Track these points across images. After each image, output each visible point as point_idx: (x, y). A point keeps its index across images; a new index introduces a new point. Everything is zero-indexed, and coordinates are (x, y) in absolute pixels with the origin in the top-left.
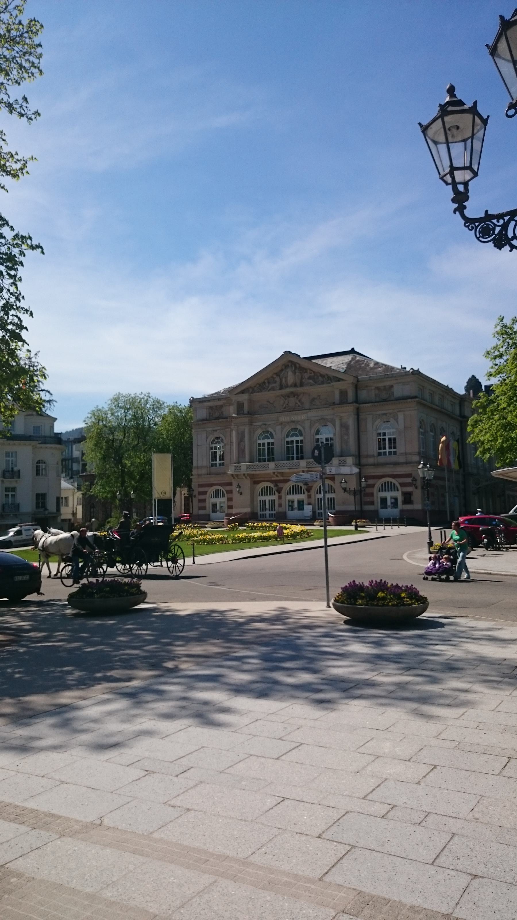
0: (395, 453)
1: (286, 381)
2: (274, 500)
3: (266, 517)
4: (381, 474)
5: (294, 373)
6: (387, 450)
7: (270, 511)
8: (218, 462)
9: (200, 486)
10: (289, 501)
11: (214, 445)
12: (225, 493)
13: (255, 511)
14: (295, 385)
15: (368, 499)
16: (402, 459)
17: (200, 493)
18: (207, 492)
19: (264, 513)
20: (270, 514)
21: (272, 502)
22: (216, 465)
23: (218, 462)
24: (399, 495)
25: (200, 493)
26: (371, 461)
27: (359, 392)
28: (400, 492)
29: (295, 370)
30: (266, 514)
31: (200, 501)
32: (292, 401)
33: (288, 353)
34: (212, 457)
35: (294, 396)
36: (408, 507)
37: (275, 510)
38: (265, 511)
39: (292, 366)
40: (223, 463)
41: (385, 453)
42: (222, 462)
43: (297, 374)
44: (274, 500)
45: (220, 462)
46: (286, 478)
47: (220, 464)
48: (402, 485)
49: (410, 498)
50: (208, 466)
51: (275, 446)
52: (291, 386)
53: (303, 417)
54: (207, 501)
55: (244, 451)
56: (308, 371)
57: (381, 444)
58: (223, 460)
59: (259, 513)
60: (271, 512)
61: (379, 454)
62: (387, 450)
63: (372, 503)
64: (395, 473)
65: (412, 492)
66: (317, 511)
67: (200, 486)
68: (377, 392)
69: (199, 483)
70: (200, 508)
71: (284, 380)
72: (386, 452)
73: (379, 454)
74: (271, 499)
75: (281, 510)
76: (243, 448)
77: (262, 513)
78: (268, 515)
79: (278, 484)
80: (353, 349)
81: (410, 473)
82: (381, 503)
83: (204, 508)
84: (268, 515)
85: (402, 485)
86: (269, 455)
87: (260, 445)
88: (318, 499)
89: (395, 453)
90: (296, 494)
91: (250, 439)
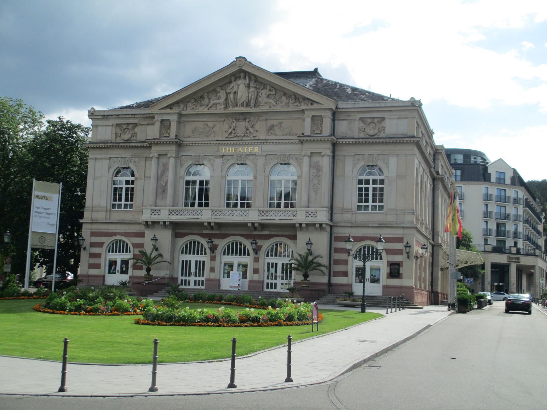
0: (381, 208)
1: (235, 98)
2: (204, 262)
3: (189, 284)
4: (361, 235)
5: (248, 87)
6: (370, 203)
7: (196, 276)
8: (123, 202)
9: (93, 234)
10: (225, 265)
12: (130, 245)
13: (175, 276)
14: (248, 105)
15: (340, 268)
16: (391, 219)
17: (93, 245)
18: (103, 243)
19: (187, 278)
20: (195, 281)
21: (200, 265)
22: (120, 206)
23: (123, 202)
24: (382, 265)
25: (93, 245)
26: (347, 217)
27: (336, 122)
28: (385, 261)
29: (249, 84)
30: (189, 281)
31: (92, 255)
32: (241, 126)
33: (241, 59)
34: (115, 194)
35: (245, 120)
37: (203, 276)
38: (189, 276)
39: (245, 78)
40: (131, 205)
41: (367, 207)
42: (129, 203)
43: (252, 89)
44: (204, 262)
45: (126, 203)
46: (223, 232)
47: (126, 206)
48: (389, 252)
49: (399, 270)
50: (108, 208)
51: (210, 186)
52: (242, 105)
53: (256, 150)
54: (103, 256)
55: (164, 191)
56: (268, 87)
57: (363, 195)
58: (132, 200)
59: (180, 278)
60: (197, 278)
61: (359, 208)
62: (370, 203)
63: (345, 274)
65: (402, 262)
66: (266, 281)
67: (93, 234)
68: (361, 124)
69: (93, 231)
70: (91, 266)
71: (232, 96)
72: (368, 206)
73: (359, 208)
74: (198, 260)
75: (213, 276)
76: (164, 185)
77: (184, 278)
78: (192, 283)
79: (213, 240)
80: (316, 70)
81: (401, 236)
82: (357, 275)
83: (98, 266)
84: (192, 283)
85: (389, 252)
86: (200, 198)
87: (188, 183)
88: (268, 264)
89: (381, 208)
90: (236, 253)
91: (176, 173)
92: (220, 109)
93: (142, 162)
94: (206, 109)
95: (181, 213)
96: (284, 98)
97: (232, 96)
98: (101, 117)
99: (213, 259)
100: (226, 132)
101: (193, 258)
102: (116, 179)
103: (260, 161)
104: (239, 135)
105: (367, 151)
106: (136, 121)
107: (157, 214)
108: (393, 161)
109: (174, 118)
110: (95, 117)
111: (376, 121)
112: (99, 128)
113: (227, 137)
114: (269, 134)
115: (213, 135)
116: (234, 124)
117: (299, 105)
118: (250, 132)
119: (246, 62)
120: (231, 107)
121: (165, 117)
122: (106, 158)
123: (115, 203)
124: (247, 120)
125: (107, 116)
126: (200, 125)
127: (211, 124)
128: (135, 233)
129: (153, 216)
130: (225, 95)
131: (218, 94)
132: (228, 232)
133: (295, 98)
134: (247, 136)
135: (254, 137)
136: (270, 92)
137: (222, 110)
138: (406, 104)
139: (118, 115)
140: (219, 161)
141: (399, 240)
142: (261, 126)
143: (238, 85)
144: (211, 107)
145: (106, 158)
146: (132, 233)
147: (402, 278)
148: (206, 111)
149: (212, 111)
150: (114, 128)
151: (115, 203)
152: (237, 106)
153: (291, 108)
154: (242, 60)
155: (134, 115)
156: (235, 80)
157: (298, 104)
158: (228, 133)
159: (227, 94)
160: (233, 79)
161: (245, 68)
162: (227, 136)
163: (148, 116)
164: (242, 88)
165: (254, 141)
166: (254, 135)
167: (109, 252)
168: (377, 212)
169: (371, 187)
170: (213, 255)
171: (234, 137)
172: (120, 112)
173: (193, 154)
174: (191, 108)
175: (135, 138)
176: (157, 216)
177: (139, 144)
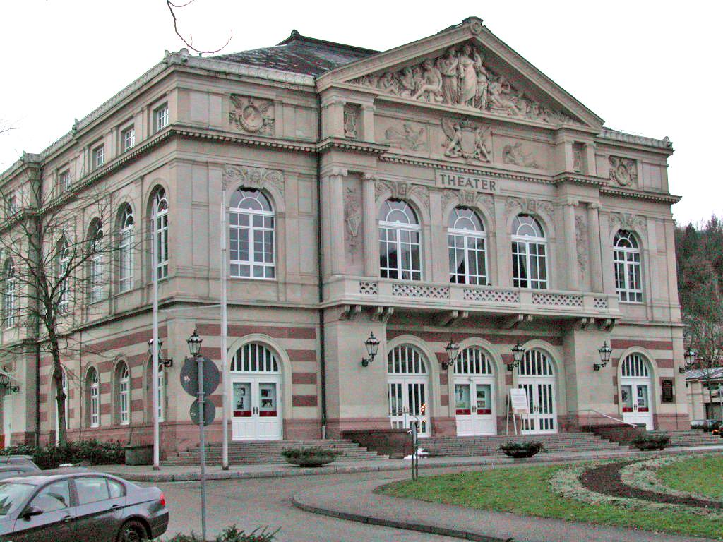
4: (628, 339)
8: (251, 262)
11: (239, 210)
23: (251, 262)
36: (667, 409)
40: (272, 271)
56: (502, 79)
64: (648, 339)
65: (674, 378)
81: (670, 340)
92: (435, 102)
93: (292, 182)
94: (414, 98)
95: (509, 297)
96: (523, 104)
97: (455, 81)
98: (203, 73)
99: (444, 380)
100: (443, 146)
101: (406, 379)
102: (233, 210)
103: (500, 206)
104: (466, 155)
105: (627, 209)
106: (270, 94)
107: (371, 291)
108: (651, 225)
109: (367, 103)
110: (188, 70)
111: (625, 163)
112: (193, 96)
113: (449, 157)
114: (507, 160)
115: (422, 147)
116: (458, 134)
117: (548, 119)
118: (482, 152)
119: (483, 29)
120: (450, 101)
121: (354, 100)
122: (215, 164)
123: (234, 262)
124: (478, 131)
125: (217, 72)
126: (398, 125)
127: (416, 127)
128: (289, 329)
129: (364, 295)
130: (441, 78)
131: (426, 74)
132: (463, 331)
133: (540, 108)
134: (478, 159)
135: (488, 162)
136: (503, 89)
137: (439, 104)
138: (655, 144)
139: (240, 76)
140: (436, 198)
141: (668, 346)
142: (494, 145)
143: (465, 66)
144: (420, 96)
145: (215, 164)
146: (285, 328)
147: (675, 403)
148: (413, 100)
149: (422, 102)
150: (228, 101)
151: (234, 262)
152: (458, 102)
153: (538, 121)
154: (479, 23)
155: (274, 81)
156: (456, 56)
157: (546, 117)
158: (449, 149)
159: (444, 76)
160: (453, 52)
161: (481, 39)
162: (448, 153)
163: (301, 89)
164: (471, 70)
165: (491, 171)
166: (488, 159)
167: (232, 369)
168: (636, 302)
169: (626, 263)
170: (444, 372)
171: (458, 157)
172: (223, 67)
173: (394, 179)
174: (389, 89)
175: (268, 129)
176: (371, 296)
177: (291, 145)
